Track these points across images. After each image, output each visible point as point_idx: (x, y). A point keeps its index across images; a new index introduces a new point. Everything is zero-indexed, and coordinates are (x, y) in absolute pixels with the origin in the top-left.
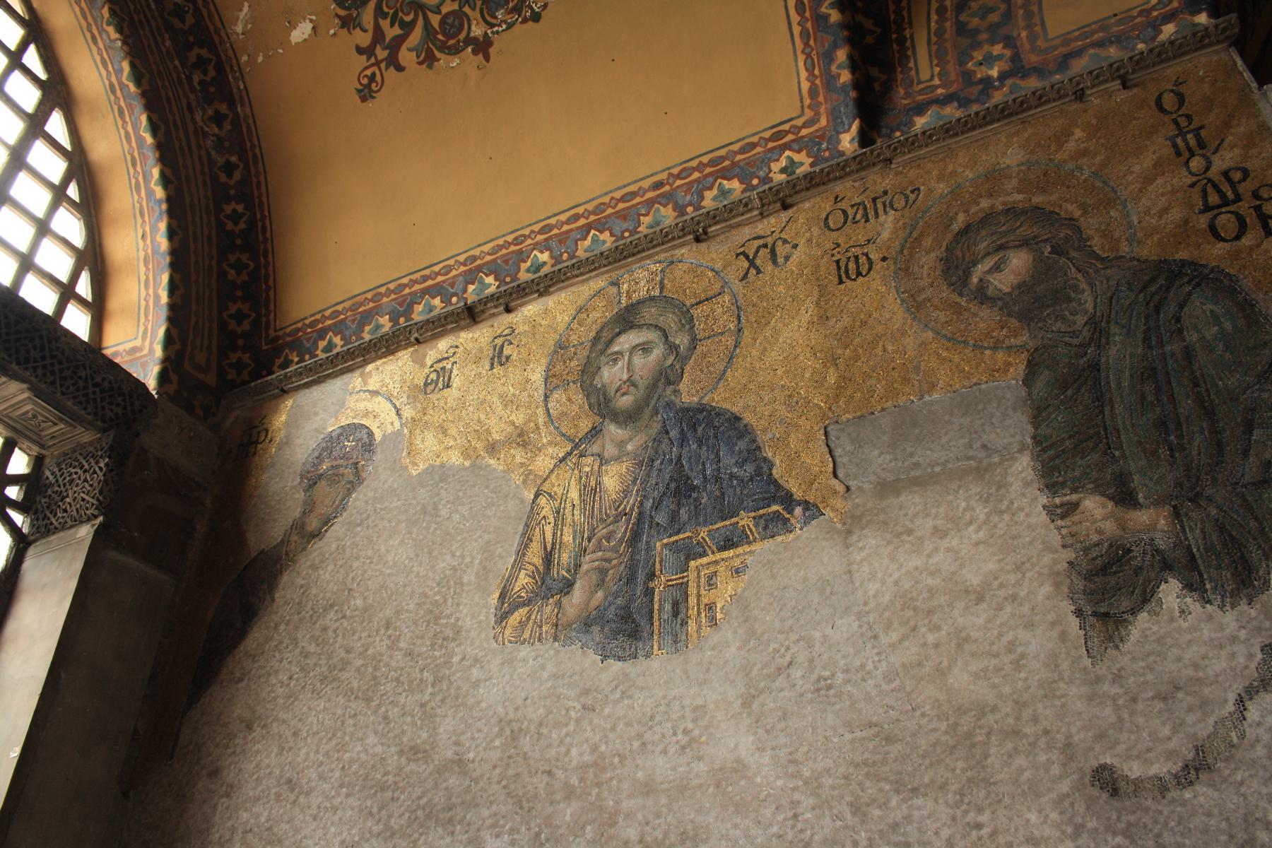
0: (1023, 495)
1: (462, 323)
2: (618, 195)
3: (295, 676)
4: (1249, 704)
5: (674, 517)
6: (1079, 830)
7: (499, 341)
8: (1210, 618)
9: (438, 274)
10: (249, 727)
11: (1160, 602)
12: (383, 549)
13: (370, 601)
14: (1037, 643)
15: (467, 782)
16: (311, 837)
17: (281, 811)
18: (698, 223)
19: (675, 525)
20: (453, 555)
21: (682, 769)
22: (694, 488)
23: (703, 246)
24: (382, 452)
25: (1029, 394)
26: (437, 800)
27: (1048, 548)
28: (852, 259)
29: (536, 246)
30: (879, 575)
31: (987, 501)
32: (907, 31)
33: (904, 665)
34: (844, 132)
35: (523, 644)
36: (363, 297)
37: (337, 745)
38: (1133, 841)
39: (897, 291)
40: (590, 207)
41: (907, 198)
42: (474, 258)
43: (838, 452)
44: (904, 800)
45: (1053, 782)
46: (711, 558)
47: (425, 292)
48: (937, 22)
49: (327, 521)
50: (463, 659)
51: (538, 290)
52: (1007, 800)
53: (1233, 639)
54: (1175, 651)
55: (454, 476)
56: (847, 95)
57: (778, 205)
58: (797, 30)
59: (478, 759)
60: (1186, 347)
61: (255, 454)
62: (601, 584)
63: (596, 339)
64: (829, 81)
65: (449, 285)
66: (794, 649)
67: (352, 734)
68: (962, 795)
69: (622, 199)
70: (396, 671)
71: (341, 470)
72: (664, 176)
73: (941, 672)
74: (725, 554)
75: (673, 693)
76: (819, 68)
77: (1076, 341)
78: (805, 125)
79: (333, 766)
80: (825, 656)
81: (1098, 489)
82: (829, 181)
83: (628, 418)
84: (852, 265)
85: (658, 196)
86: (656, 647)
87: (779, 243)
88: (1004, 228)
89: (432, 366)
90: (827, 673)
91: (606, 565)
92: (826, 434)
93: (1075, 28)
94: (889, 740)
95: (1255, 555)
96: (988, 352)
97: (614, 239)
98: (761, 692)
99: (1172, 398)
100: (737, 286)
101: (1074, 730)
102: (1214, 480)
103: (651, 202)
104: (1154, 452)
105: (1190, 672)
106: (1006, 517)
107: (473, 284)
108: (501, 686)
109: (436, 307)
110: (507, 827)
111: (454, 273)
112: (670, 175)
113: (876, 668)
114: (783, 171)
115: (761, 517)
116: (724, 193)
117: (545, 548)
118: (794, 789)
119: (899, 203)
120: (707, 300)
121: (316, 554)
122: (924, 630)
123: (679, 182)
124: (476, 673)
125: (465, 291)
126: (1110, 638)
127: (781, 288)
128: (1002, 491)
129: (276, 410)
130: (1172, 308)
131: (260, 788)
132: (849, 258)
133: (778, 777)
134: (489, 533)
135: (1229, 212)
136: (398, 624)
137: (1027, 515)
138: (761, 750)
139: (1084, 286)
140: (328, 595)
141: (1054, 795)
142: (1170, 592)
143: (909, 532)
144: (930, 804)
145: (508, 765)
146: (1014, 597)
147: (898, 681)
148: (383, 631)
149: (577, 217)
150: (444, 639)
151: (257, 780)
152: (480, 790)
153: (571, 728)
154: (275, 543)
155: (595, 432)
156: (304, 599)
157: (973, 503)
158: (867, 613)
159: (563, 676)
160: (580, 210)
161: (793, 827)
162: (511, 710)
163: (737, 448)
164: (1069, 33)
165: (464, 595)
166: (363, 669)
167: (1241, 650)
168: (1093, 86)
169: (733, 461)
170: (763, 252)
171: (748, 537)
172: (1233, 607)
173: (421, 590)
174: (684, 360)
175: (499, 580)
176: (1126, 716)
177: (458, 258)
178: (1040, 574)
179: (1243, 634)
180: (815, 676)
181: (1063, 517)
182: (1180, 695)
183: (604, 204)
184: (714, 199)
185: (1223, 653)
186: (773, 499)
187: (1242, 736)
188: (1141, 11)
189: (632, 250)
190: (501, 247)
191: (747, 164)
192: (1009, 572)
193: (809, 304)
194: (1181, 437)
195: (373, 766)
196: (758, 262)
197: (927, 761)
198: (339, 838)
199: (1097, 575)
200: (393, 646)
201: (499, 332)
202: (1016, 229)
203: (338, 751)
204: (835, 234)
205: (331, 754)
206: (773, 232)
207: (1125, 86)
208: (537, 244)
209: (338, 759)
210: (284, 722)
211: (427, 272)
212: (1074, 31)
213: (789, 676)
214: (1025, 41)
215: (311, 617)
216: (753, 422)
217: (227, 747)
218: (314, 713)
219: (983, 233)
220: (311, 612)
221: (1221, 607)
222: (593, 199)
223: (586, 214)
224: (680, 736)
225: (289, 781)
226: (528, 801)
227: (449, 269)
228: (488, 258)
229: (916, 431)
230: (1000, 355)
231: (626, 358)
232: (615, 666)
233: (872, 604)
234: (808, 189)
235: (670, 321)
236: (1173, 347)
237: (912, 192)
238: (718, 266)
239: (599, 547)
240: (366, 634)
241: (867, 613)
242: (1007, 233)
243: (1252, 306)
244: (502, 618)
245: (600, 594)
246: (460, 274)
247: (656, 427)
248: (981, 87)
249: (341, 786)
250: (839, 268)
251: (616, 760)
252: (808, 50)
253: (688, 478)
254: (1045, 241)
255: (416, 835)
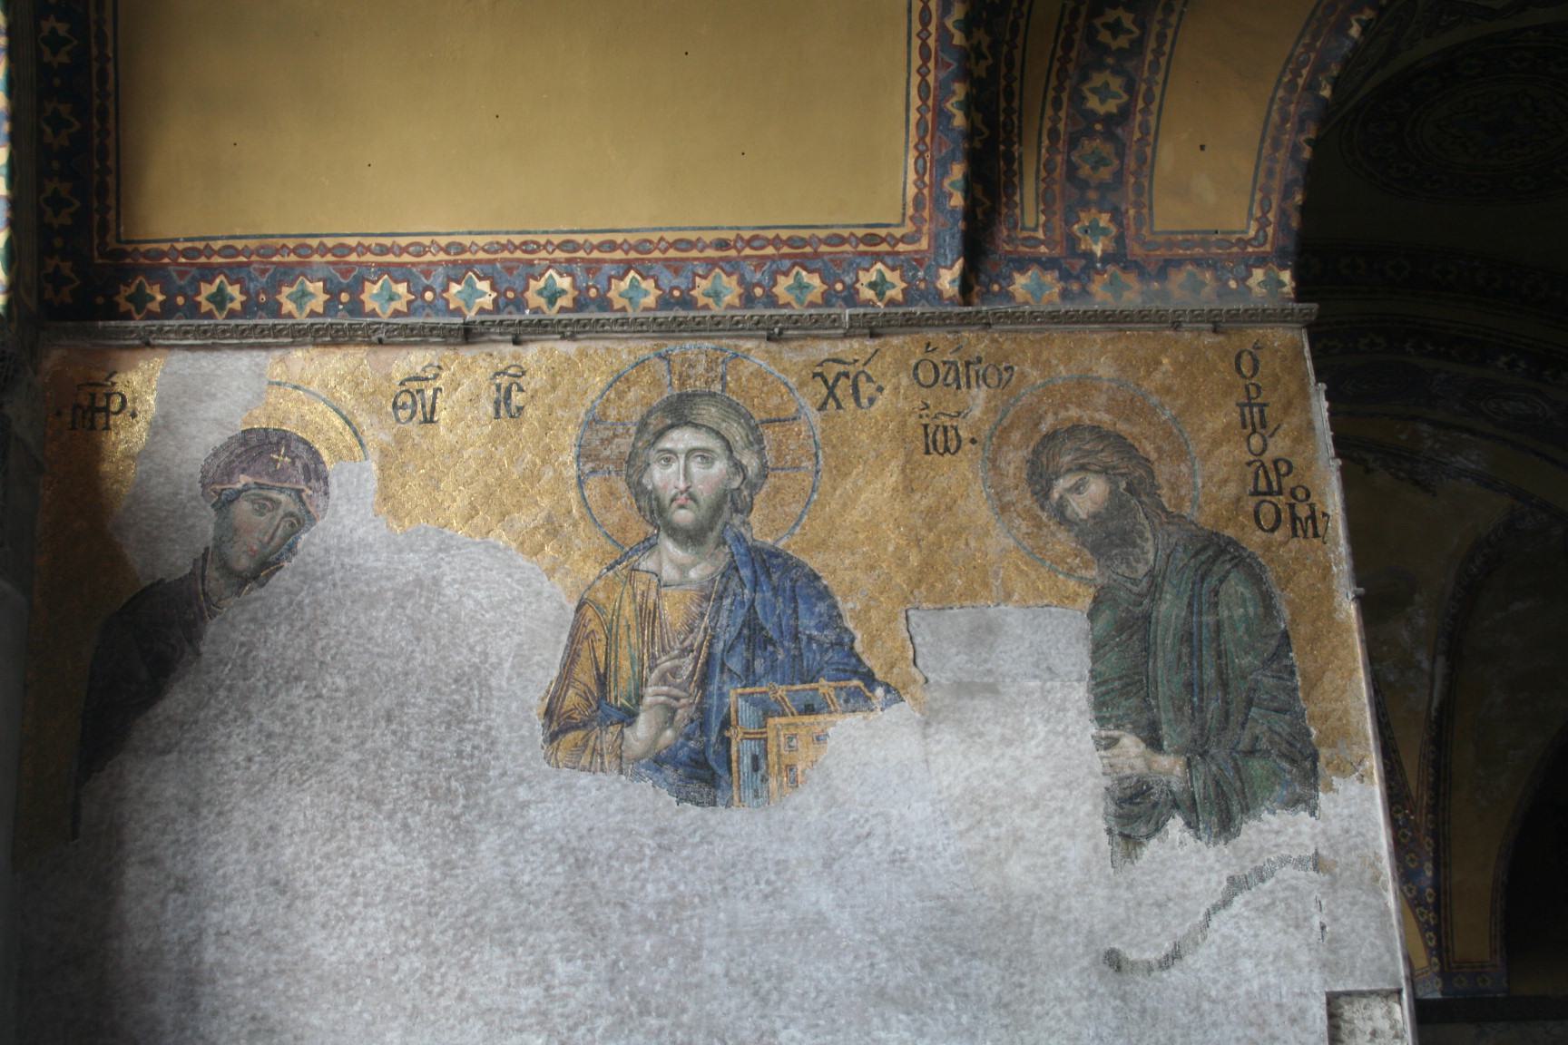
0: (1078, 722)
1: (452, 340)
2: (671, 237)
3: (257, 759)
4: (1213, 917)
5: (748, 667)
6: (1092, 993)
7: (504, 381)
8: (1199, 851)
9: (404, 250)
10: (194, 810)
11: (1167, 833)
12: (363, 620)
13: (357, 682)
14: (1076, 851)
15: (524, 905)
16: (322, 945)
17: (271, 915)
18: (777, 322)
19: (749, 677)
20: (472, 649)
21: (766, 915)
22: (770, 641)
23: (773, 347)
24: (340, 486)
25: (1092, 629)
26: (487, 919)
27: (1091, 773)
28: (941, 429)
29: (553, 263)
30: (953, 769)
31: (1048, 721)
32: (1016, 146)
33: (969, 852)
34: (945, 267)
35: (583, 769)
36: (281, 241)
37: (339, 848)
38: (1126, 1004)
39: (984, 483)
40: (633, 238)
41: (1000, 374)
42: (462, 249)
43: (918, 640)
44: (965, 961)
45: (1078, 958)
46: (790, 719)
47: (384, 268)
48: (1048, 151)
49: (265, 567)
50: (504, 774)
51: (563, 333)
52: (1043, 968)
53: (1211, 869)
54: (1172, 872)
55: (459, 549)
56: (955, 223)
57: (867, 331)
58: (914, 116)
59: (536, 882)
60: (1218, 621)
61: (107, 428)
62: (670, 721)
63: (643, 425)
64: (939, 198)
65: (422, 272)
66: (873, 822)
67: (360, 839)
68: (1011, 961)
69: (675, 245)
70: (410, 774)
71: (274, 494)
72: (731, 235)
73: (1000, 862)
74: (806, 719)
75: (756, 844)
76: (931, 175)
77: (1135, 589)
78: (903, 239)
79: (339, 871)
80: (901, 833)
81: (1136, 729)
82: (926, 325)
83: (692, 537)
84: (940, 437)
85: (721, 259)
86: (736, 798)
87: (862, 378)
88: (1087, 447)
89: (402, 384)
90: (901, 848)
91: (674, 703)
92: (907, 618)
93: (1179, 229)
94: (954, 911)
95: (1236, 808)
96: (1061, 577)
97: (659, 292)
98: (842, 856)
99: (1200, 666)
100: (814, 416)
101: (1096, 921)
102: (1219, 742)
103: (712, 263)
104: (1180, 709)
105: (1179, 889)
106: (1062, 739)
107: (459, 282)
108: (557, 812)
109: (400, 297)
110: (580, 952)
111: (428, 258)
112: (739, 237)
113: (945, 850)
114: (872, 285)
115: (841, 689)
116: (801, 287)
117: (598, 669)
118: (871, 943)
119: (993, 381)
120: (779, 421)
121: (258, 604)
122: (987, 824)
123: (748, 251)
124: (522, 793)
125: (446, 289)
126: (1129, 856)
127: (864, 436)
128: (1061, 714)
129: (133, 367)
130: (1213, 581)
131: (230, 887)
132: (938, 427)
133: (856, 931)
134: (520, 634)
135: (1270, 502)
136: (405, 719)
137: (1078, 741)
138: (841, 907)
139: (1148, 535)
140: (288, 663)
141: (1077, 968)
142: (1176, 826)
143: (981, 735)
144: (986, 966)
145: (573, 893)
146: (1062, 810)
147: (963, 865)
148: (383, 724)
149: (613, 246)
150: (474, 747)
151: (224, 876)
152: (543, 914)
153: (646, 864)
154: (181, 575)
155: (649, 545)
156: (250, 663)
157: (1036, 719)
158: (941, 801)
159: (634, 811)
160: (619, 238)
161: (870, 974)
162: (573, 837)
163: (817, 610)
164: (1172, 233)
165: (495, 701)
166: (362, 764)
167: (1214, 877)
168: (1190, 322)
169: (813, 623)
170: (843, 381)
171: (829, 706)
172: (1215, 844)
173: (431, 683)
174: (754, 488)
175: (543, 693)
176: (1132, 915)
177: (437, 239)
178: (1084, 794)
179: (1217, 866)
180: (890, 849)
181: (1106, 748)
182: (1171, 905)
183: (650, 242)
184: (789, 289)
185: (1203, 879)
186: (855, 673)
187: (1205, 938)
188: (1239, 240)
189: (693, 325)
190: (504, 247)
191: (832, 260)
192: (1059, 787)
193: (895, 466)
194: (1201, 700)
195: (396, 877)
196: (838, 392)
197: (985, 932)
198: (363, 950)
199: (1125, 801)
200: (403, 741)
201: (501, 367)
202: (1098, 452)
203: (343, 856)
204: (924, 391)
205: (334, 857)
206: (856, 361)
207: (1215, 331)
208: (554, 261)
209: (344, 864)
210: (250, 812)
211: (388, 241)
212: (1177, 233)
213: (867, 845)
214: (1132, 222)
215: (267, 686)
216: (833, 587)
217: (164, 832)
218: (296, 808)
219: (1069, 445)
220: (265, 681)
221: (1207, 844)
222: (637, 230)
223: (626, 247)
224: (763, 886)
225: (276, 883)
226: (601, 929)
227: (423, 250)
228: (481, 255)
229: (992, 638)
230: (1072, 583)
231: (682, 461)
232: (693, 811)
233: (945, 794)
234: (901, 326)
235: (736, 432)
236: (1208, 619)
237: (1006, 369)
238: (792, 381)
239: (663, 680)
240: (359, 723)
241: (941, 801)
242: (1088, 453)
243: (1271, 598)
244: (553, 738)
245: (669, 733)
246: (439, 263)
247: (723, 560)
248: (1083, 262)
249: (356, 894)
250: (927, 435)
251: (696, 900)
252: (922, 147)
253: (763, 628)
254: (1122, 475)
255: (466, 954)
